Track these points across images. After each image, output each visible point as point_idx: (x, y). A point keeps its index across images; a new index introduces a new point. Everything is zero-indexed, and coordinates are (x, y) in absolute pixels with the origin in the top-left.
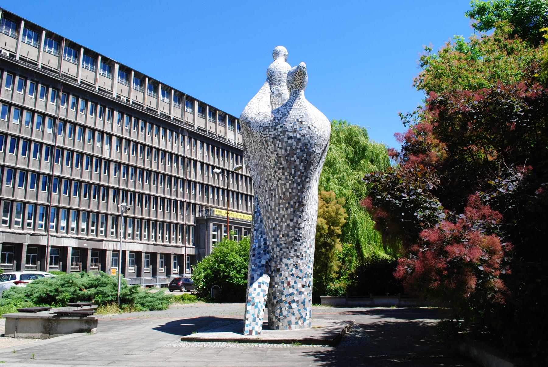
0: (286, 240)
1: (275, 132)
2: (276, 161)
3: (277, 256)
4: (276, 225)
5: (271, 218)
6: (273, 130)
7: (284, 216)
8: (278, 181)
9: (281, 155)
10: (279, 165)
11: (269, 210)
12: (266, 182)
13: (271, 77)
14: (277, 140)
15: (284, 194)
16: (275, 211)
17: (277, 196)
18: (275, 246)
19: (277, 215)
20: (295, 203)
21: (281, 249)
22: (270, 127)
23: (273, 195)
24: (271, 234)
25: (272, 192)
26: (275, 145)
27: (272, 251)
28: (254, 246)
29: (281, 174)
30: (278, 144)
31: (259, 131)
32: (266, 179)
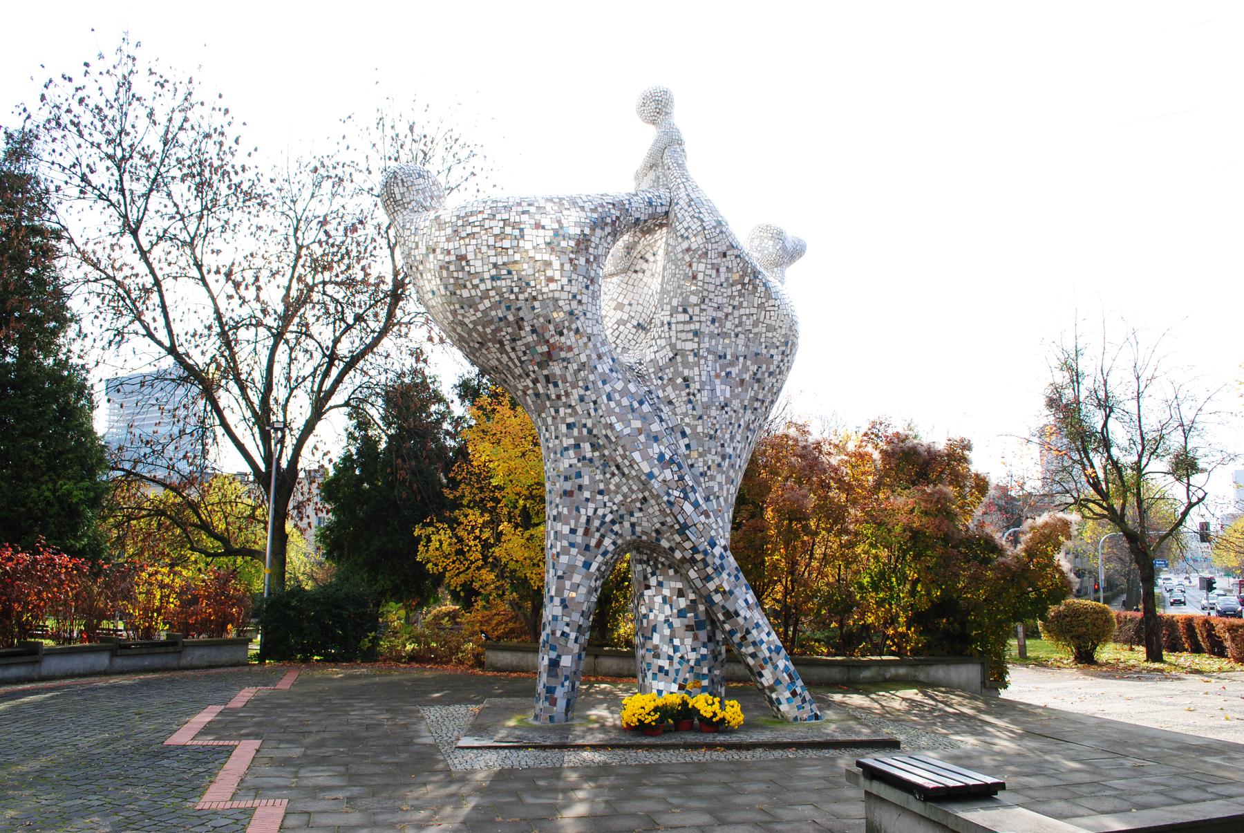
25: (749, 434)
32: (746, 403)
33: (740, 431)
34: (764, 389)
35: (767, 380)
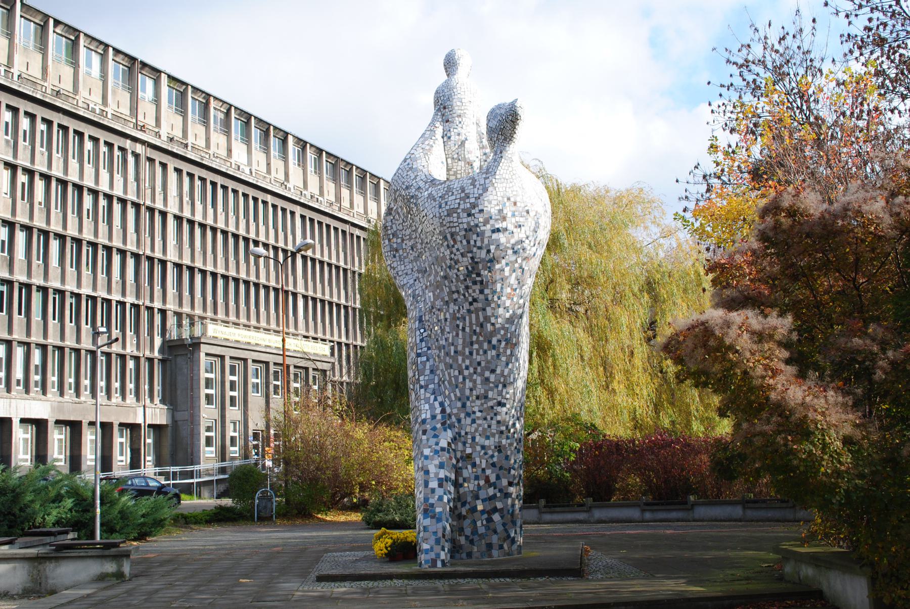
0: (482, 404)
1: (469, 219)
2: (470, 269)
3: (466, 433)
4: (464, 379)
5: (455, 366)
6: (465, 215)
7: (479, 364)
8: (471, 304)
9: (479, 260)
10: (474, 276)
11: (452, 353)
12: (447, 303)
13: (445, 108)
14: (474, 234)
15: (482, 326)
16: (463, 354)
17: (467, 330)
18: (462, 415)
19: (467, 362)
20: (499, 341)
21: (474, 421)
22: (459, 211)
23: (461, 328)
24: (455, 395)
25: (458, 322)
26: (468, 242)
27: (456, 424)
28: (423, 416)
29: (478, 292)
30: (475, 241)
31: (438, 215)
32: (446, 299)
33: (448, 323)
34: (452, 282)
35: (451, 274)
